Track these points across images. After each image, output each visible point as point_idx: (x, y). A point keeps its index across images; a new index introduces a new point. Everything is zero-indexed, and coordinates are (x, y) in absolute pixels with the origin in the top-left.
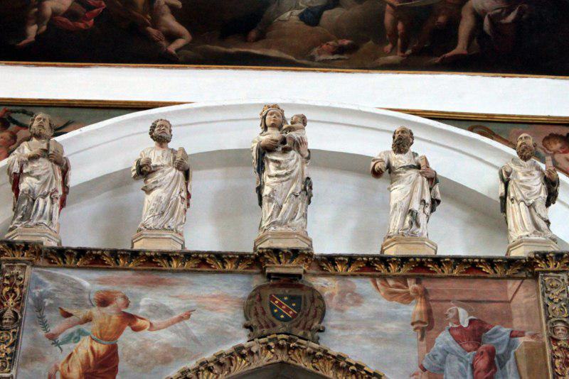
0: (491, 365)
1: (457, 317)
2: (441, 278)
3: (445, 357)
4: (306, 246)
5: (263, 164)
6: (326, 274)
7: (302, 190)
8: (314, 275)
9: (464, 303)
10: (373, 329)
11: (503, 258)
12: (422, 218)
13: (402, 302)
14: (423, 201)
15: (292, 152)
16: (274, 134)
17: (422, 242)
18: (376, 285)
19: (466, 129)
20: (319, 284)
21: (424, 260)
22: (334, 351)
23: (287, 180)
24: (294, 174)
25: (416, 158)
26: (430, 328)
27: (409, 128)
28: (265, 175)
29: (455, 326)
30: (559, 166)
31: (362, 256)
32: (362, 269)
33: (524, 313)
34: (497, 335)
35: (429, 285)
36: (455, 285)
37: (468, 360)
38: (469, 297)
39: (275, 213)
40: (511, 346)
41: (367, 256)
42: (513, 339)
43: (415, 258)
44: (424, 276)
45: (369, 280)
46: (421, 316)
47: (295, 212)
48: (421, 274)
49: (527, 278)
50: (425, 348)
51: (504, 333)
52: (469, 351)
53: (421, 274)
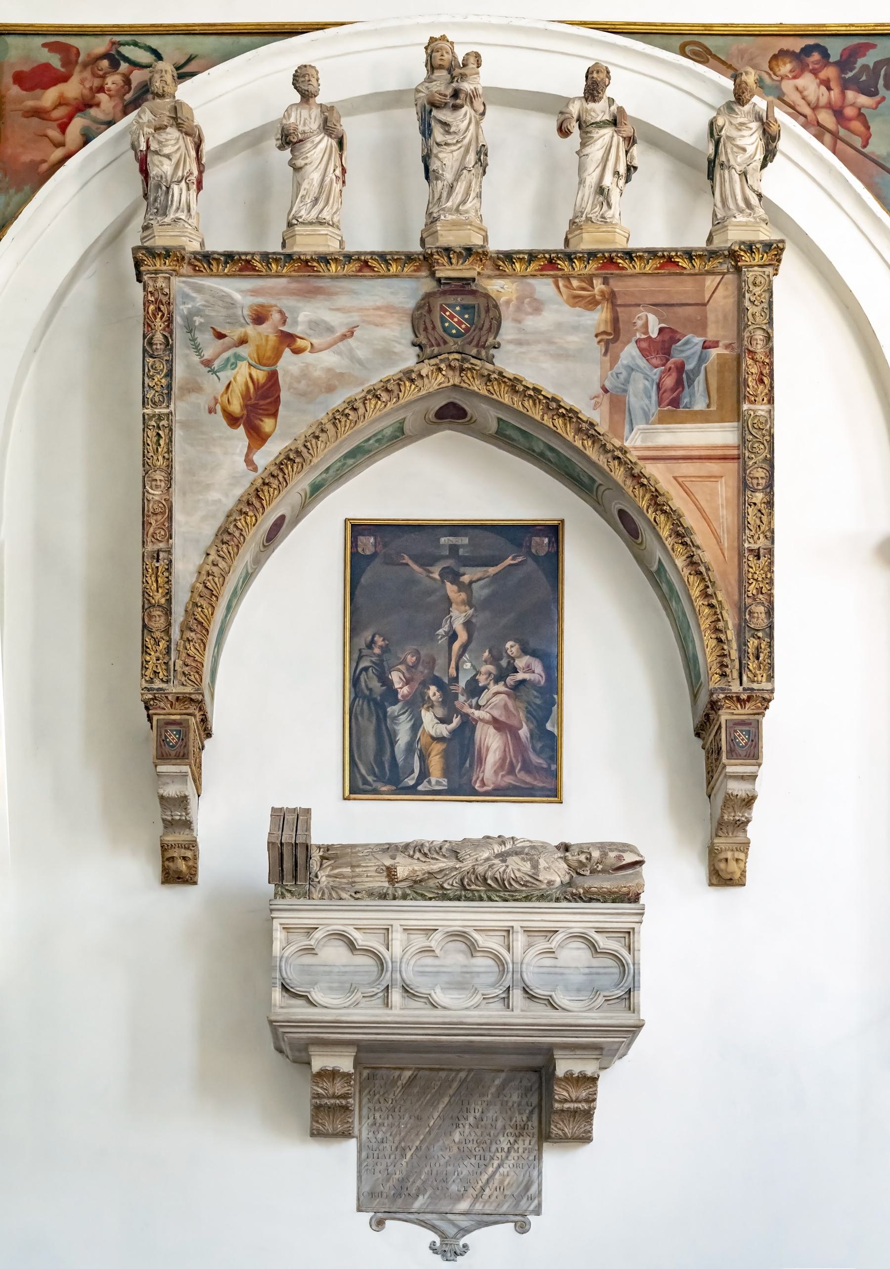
0: (679, 383)
1: (646, 325)
3: (629, 375)
5: (430, 125)
6: (503, 275)
7: (476, 163)
8: (489, 277)
11: (703, 250)
12: (615, 197)
14: (616, 173)
18: (558, 287)
20: (497, 288)
22: (511, 371)
24: (466, 141)
26: (616, 339)
28: (431, 142)
29: (643, 336)
33: (721, 317)
35: (617, 286)
36: (645, 284)
38: (661, 299)
39: (445, 195)
40: (702, 359)
42: (705, 351)
43: (603, 252)
45: (550, 281)
47: (467, 194)
48: (609, 272)
49: (728, 272)
51: (696, 344)
53: (609, 272)
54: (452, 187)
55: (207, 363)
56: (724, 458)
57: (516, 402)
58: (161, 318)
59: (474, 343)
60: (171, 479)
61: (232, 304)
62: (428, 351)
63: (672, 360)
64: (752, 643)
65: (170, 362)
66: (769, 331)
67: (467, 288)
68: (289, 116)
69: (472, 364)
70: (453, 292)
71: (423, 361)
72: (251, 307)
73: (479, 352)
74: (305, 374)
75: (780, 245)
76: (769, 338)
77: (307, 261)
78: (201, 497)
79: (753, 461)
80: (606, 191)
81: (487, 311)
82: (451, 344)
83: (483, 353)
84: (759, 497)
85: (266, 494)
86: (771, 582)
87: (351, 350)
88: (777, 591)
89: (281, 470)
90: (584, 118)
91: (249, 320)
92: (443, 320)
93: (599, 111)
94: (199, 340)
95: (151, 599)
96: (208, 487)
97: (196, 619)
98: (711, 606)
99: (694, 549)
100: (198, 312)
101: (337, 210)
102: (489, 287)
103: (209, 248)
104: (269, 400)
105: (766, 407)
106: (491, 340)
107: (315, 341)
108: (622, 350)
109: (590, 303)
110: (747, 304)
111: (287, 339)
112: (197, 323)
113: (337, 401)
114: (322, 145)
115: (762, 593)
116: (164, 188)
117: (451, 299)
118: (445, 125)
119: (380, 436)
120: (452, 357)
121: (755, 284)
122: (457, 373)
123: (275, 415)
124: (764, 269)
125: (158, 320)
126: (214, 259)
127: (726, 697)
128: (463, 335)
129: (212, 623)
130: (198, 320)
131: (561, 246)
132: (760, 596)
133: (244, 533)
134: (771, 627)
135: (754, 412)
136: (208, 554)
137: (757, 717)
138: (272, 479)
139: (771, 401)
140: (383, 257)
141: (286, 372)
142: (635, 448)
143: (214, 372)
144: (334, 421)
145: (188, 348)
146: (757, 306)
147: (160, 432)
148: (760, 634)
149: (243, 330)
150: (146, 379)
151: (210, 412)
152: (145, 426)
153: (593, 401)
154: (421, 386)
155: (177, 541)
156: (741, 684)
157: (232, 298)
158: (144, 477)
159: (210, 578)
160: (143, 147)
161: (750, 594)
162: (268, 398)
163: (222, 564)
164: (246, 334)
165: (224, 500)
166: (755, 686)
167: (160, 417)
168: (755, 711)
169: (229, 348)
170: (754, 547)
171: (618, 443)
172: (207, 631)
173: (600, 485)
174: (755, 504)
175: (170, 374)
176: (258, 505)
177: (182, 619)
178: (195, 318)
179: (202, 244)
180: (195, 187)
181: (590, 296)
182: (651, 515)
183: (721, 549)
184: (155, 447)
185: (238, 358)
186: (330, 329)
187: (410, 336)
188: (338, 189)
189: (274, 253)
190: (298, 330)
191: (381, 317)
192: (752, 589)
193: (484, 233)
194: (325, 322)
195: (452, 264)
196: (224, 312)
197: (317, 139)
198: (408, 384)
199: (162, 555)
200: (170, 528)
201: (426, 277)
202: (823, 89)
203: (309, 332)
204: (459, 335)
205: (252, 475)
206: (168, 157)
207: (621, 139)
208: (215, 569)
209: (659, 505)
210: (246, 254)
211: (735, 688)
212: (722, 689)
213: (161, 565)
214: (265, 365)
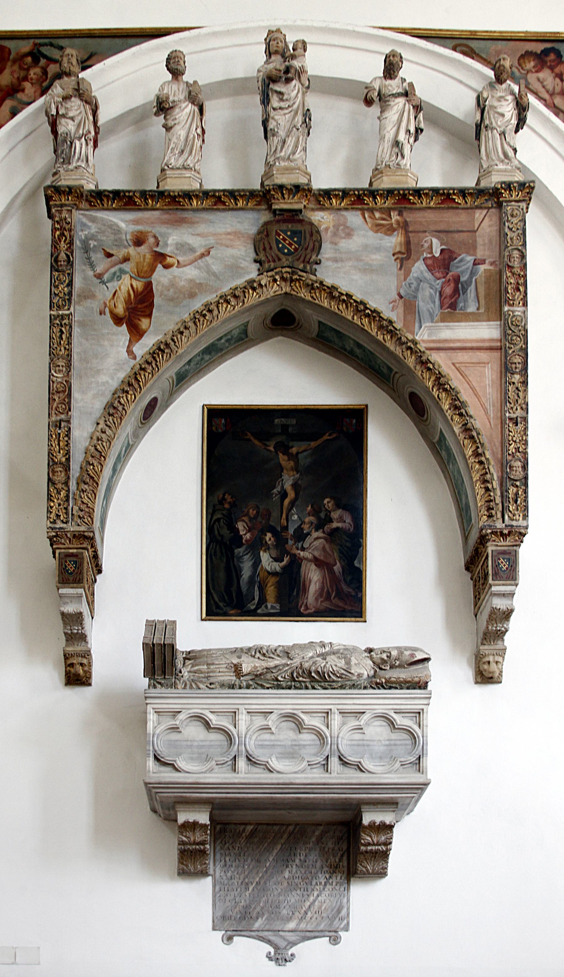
0: (456, 291)
1: (431, 247)
2: (420, 209)
3: (419, 285)
4: (306, 181)
5: (268, 95)
6: (322, 208)
7: (303, 123)
8: (313, 210)
9: (438, 234)
10: (361, 260)
11: (473, 189)
12: (407, 150)
13: (386, 234)
14: (408, 131)
15: (294, 82)
16: (277, 63)
17: (405, 172)
18: (365, 218)
19: (449, 48)
20: (317, 218)
21: (407, 192)
22: (329, 282)
23: (290, 112)
24: (295, 106)
25: (404, 84)
26: (408, 258)
27: (399, 50)
28: (269, 108)
29: (429, 256)
30: (530, 87)
31: (354, 190)
32: (353, 203)
33: (487, 241)
34: (462, 263)
35: (409, 217)
36: (430, 216)
37: (438, 287)
38: (442, 227)
39: (279, 148)
40: (473, 274)
41: (358, 190)
42: (475, 267)
43: (398, 190)
44: (405, 208)
45: (359, 213)
46: (401, 247)
47: (296, 147)
48: (403, 206)
49: (492, 207)
50: (403, 277)
51: (469, 262)
52: (438, 279)
53: (403, 206)
54: (284, 142)
55: (99, 276)
56: (491, 349)
57: (334, 307)
58: (65, 241)
59: (302, 259)
60: (71, 364)
61: (117, 231)
62: (267, 266)
63: (450, 274)
64: (512, 491)
65: (71, 275)
66: (524, 251)
67: (296, 218)
68: (163, 90)
69: (300, 276)
70: (285, 221)
71: (262, 274)
72: (132, 233)
73: (305, 267)
74: (172, 284)
75: (532, 184)
76: (523, 256)
77: (175, 197)
78: (93, 380)
79: (512, 350)
80: (400, 145)
81: (312, 235)
82: (284, 260)
83: (308, 267)
84: (517, 378)
85: (143, 377)
86: (526, 443)
87: (208, 266)
88: (530, 450)
89: (154, 358)
90: (383, 92)
91: (131, 243)
92: (278, 242)
93: (394, 86)
94: (93, 259)
95: (54, 458)
96: (98, 372)
97: (89, 475)
98: (481, 463)
99: (468, 418)
100: (93, 237)
101: (198, 161)
102: (312, 218)
103: (101, 187)
104: (145, 304)
105: (521, 309)
106: (314, 257)
107: (180, 259)
108: (413, 266)
109: (388, 230)
110: (507, 230)
111: (160, 258)
112: (92, 246)
113: (198, 304)
114: (188, 110)
115: (519, 452)
116: (69, 143)
117: (284, 226)
118: (280, 93)
119: (229, 337)
120: (284, 270)
121: (512, 216)
122: (289, 284)
123: (150, 316)
124: (520, 204)
125: (62, 242)
126: (105, 196)
127: (492, 533)
128: (292, 253)
129: (101, 478)
130: (92, 243)
131: (366, 186)
132: (518, 454)
133: (126, 408)
134: (526, 478)
135: (513, 312)
136: (98, 424)
137: (515, 548)
138: (147, 366)
139: (525, 304)
140: (232, 194)
141: (159, 283)
142: (423, 341)
143: (104, 283)
144: (194, 320)
145: (85, 264)
146: (514, 232)
147: (63, 329)
148: (518, 483)
149: (126, 251)
150: (53, 288)
151: (101, 314)
152: (52, 324)
153: (391, 305)
154: (261, 293)
155: (74, 413)
156: (503, 522)
157: (118, 226)
158: (50, 364)
159: (100, 442)
160: (54, 112)
161: (510, 452)
162: (144, 303)
163: (109, 432)
164: (128, 253)
165: (110, 381)
166: (514, 523)
167: (62, 317)
168: (514, 544)
169: (116, 264)
170: (513, 415)
171: (410, 337)
172: (97, 484)
173: (396, 373)
174: (514, 383)
175: (70, 284)
176: (136, 386)
177: (78, 474)
178: (90, 242)
179: (97, 186)
180: (92, 143)
181: (388, 224)
182: (435, 393)
183: (488, 419)
184: (58, 340)
185: (122, 272)
186: (192, 250)
187: (253, 255)
188: (199, 145)
189: (151, 191)
190: (168, 251)
191: (231, 240)
192: (512, 448)
193: (308, 177)
194: (189, 244)
195: (284, 198)
196: (112, 237)
197: (184, 105)
198: (251, 291)
199: (63, 424)
200: (69, 403)
201: (266, 210)
202: (558, 80)
203: (176, 252)
204: (290, 253)
205: (132, 362)
206: (72, 119)
207: (411, 107)
208: (104, 436)
209: (441, 385)
210: (129, 191)
211: (499, 525)
212: (490, 526)
213: (62, 432)
214: (143, 277)
